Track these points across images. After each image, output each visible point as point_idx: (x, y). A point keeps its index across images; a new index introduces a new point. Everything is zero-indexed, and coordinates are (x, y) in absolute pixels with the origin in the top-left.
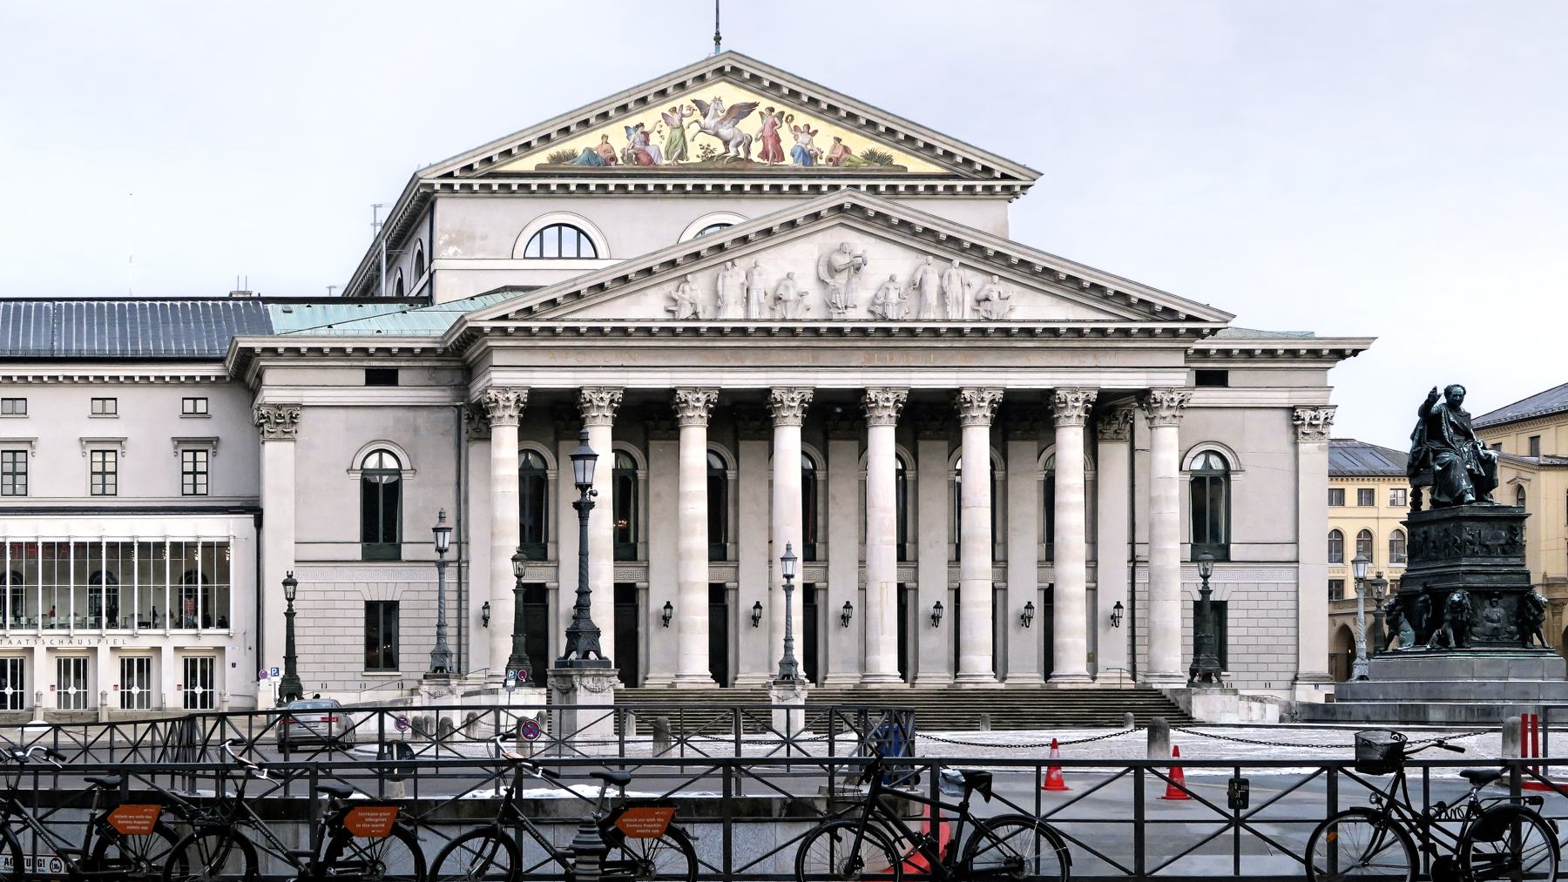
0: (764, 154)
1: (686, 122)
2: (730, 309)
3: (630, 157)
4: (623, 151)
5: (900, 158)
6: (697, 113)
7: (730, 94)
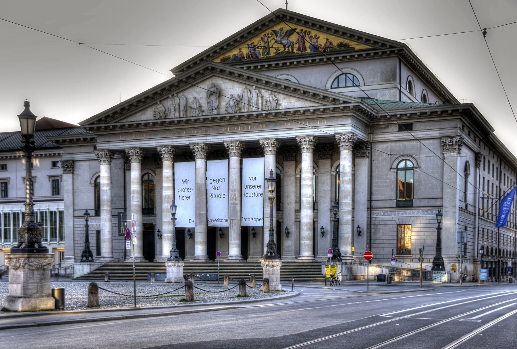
0: (299, 49)
1: (270, 39)
2: (172, 113)
4: (246, 54)
5: (352, 44)
6: (274, 35)
7: (285, 27)
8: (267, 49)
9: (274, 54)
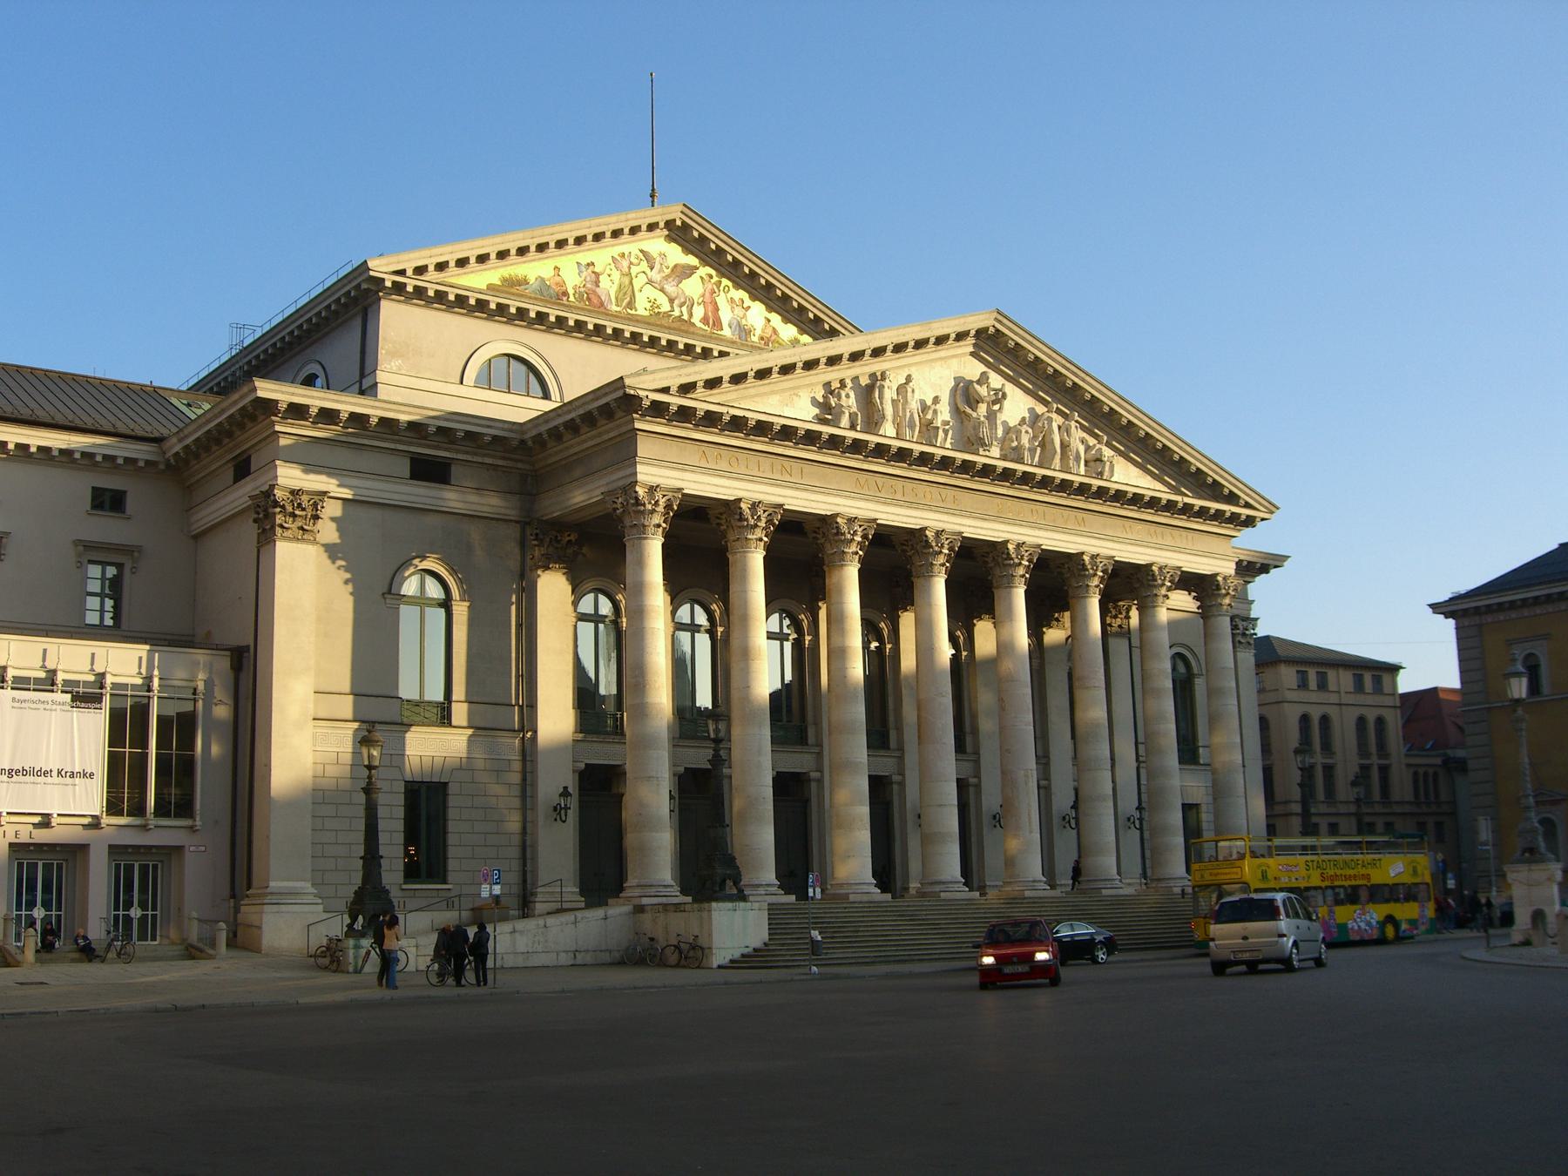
0: (705, 320)
1: (634, 270)
3: (580, 297)
4: (574, 288)
6: (644, 266)
8: (627, 294)
9: (647, 313)
